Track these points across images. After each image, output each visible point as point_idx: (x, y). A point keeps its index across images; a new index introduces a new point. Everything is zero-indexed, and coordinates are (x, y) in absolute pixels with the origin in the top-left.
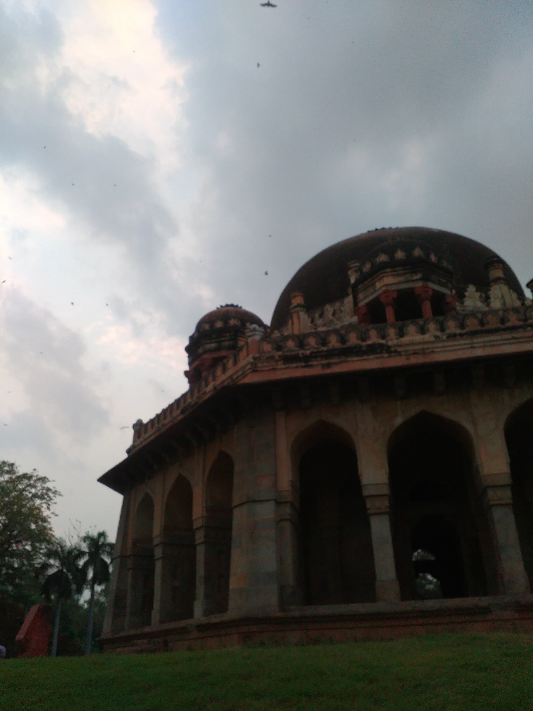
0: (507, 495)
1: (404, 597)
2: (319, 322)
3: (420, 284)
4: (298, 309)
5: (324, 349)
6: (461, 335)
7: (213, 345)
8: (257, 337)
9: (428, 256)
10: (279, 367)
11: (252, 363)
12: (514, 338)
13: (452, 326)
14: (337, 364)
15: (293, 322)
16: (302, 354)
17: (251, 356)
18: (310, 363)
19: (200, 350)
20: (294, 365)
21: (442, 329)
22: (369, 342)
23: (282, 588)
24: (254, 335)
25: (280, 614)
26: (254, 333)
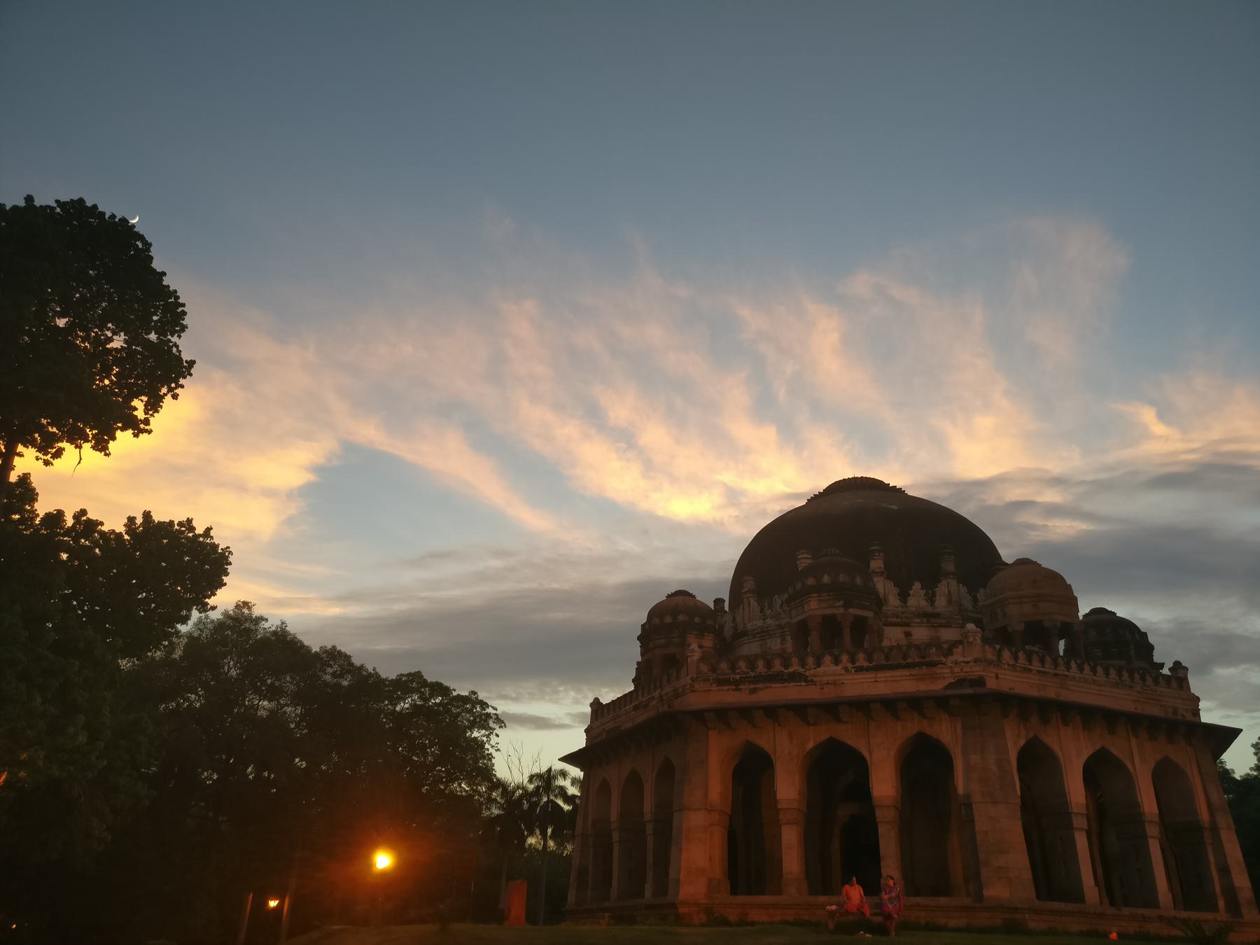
2: (768, 612)
3: (842, 610)
7: (663, 641)
8: (696, 658)
10: (714, 689)
12: (911, 675)
13: (862, 660)
15: (743, 608)
17: (690, 677)
18: (740, 687)
20: (726, 688)
21: (853, 661)
22: (791, 670)
24: (693, 655)
26: (693, 654)
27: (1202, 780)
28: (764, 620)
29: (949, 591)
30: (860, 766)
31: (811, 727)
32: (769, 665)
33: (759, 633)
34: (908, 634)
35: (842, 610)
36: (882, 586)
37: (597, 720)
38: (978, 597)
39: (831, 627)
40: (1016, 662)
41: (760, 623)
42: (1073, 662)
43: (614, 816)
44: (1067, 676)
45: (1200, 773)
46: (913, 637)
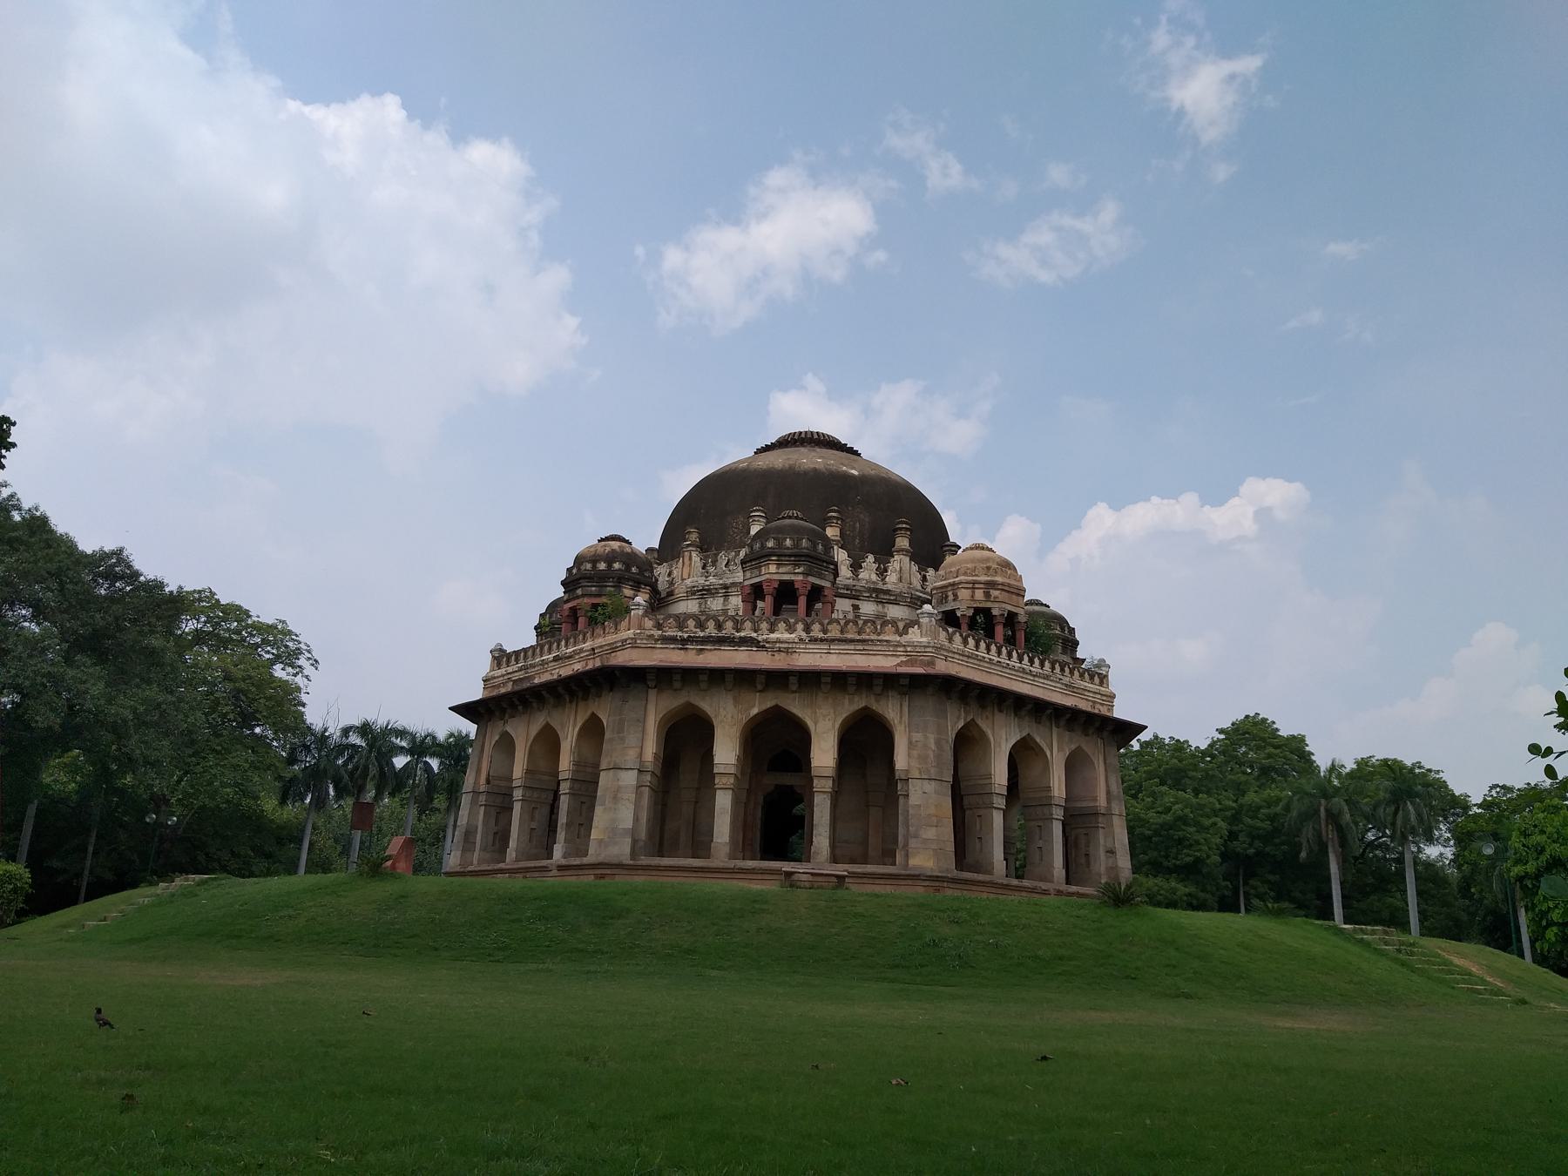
0: (828, 785)
1: (732, 857)
2: (712, 570)
3: (800, 578)
4: (690, 548)
5: (702, 634)
6: (822, 640)
9: (815, 545)
10: (658, 646)
11: (632, 639)
13: (816, 631)
19: (579, 592)
20: (672, 646)
22: (742, 634)
23: (635, 842)
25: (631, 862)
27: (1106, 770)
28: (707, 577)
29: (901, 568)
30: (802, 738)
31: (758, 694)
32: (719, 626)
33: (701, 591)
34: (856, 607)
35: (800, 578)
36: (841, 556)
37: (499, 666)
38: (928, 577)
39: (785, 595)
40: (965, 646)
41: (702, 581)
42: (1004, 648)
43: (518, 771)
44: (1008, 664)
45: (1105, 763)
46: (861, 611)
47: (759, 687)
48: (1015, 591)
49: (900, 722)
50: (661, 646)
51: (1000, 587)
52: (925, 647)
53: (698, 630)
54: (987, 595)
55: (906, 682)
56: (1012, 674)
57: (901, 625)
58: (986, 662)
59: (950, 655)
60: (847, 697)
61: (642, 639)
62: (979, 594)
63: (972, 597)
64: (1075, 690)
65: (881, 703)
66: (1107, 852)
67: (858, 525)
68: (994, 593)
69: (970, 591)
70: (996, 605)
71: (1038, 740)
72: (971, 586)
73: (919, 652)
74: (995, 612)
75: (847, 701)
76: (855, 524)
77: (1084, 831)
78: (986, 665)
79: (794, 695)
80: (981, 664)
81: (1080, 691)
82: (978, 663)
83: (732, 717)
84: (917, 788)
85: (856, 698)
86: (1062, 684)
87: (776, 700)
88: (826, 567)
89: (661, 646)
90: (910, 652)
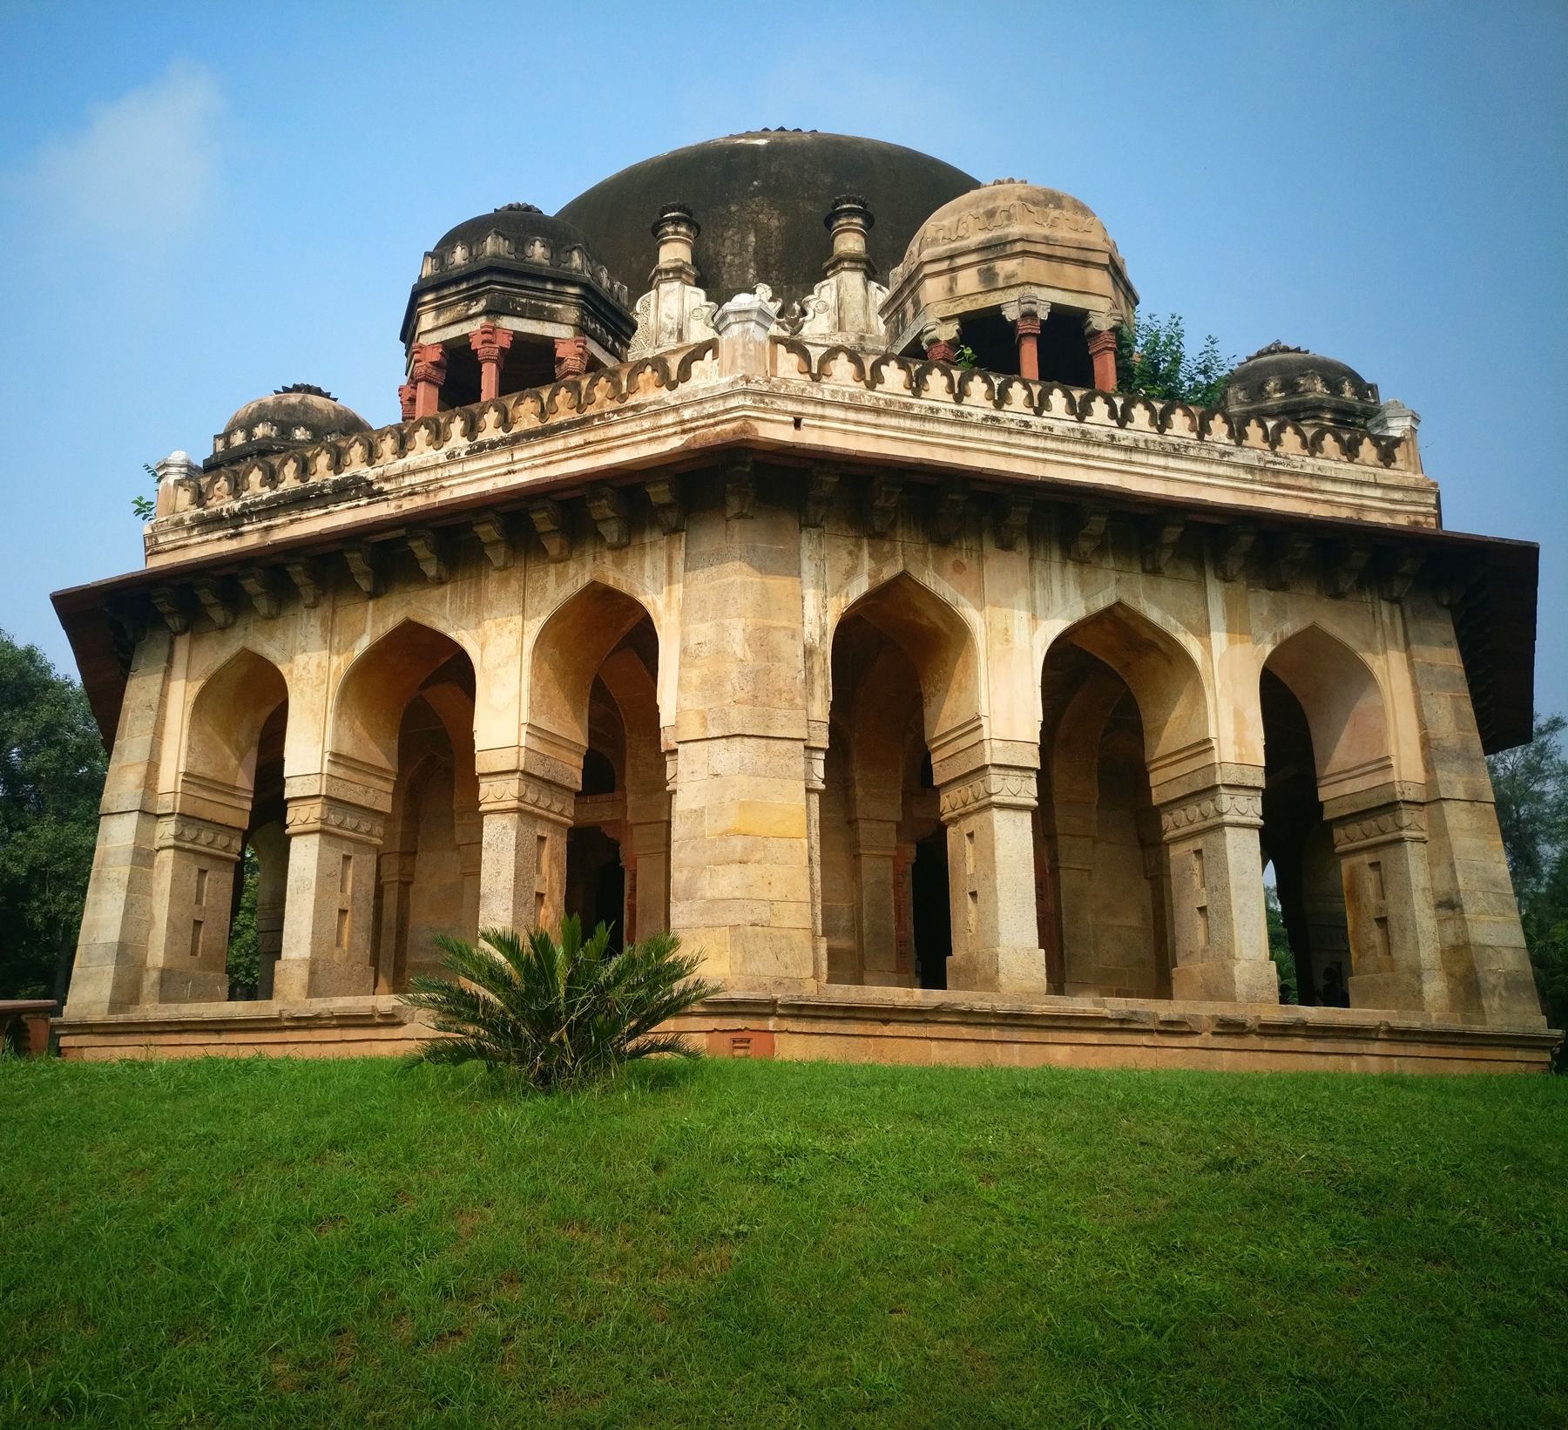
14: (284, 525)
16: (228, 509)
20: (216, 535)
31: (371, 604)
47: (365, 585)
48: (1074, 254)
49: (668, 605)
50: (199, 539)
51: (1018, 247)
52: (724, 396)
53: (267, 488)
54: (988, 277)
55: (660, 494)
56: (1045, 450)
57: (674, 363)
58: (946, 422)
59: (810, 409)
60: (552, 569)
61: (165, 533)
62: (968, 281)
63: (951, 290)
64: (1284, 480)
65: (628, 567)
66: (1439, 905)
67: (752, 238)
68: (1004, 267)
69: (944, 279)
70: (1014, 294)
71: (1154, 615)
72: (944, 265)
73: (714, 415)
74: (1011, 314)
75: (552, 579)
76: (744, 238)
77: (1367, 858)
78: (945, 429)
79: (441, 590)
80: (928, 426)
81: (1305, 482)
82: (917, 425)
83: (319, 666)
84: (696, 767)
85: (572, 568)
86: (1235, 465)
87: (405, 610)
88: (554, 292)
89: (199, 539)
90: (692, 420)
